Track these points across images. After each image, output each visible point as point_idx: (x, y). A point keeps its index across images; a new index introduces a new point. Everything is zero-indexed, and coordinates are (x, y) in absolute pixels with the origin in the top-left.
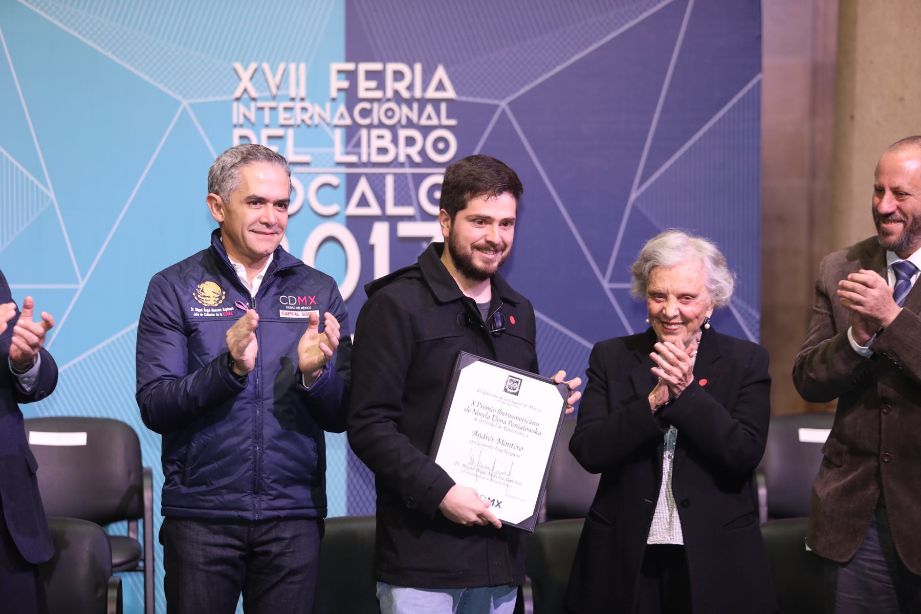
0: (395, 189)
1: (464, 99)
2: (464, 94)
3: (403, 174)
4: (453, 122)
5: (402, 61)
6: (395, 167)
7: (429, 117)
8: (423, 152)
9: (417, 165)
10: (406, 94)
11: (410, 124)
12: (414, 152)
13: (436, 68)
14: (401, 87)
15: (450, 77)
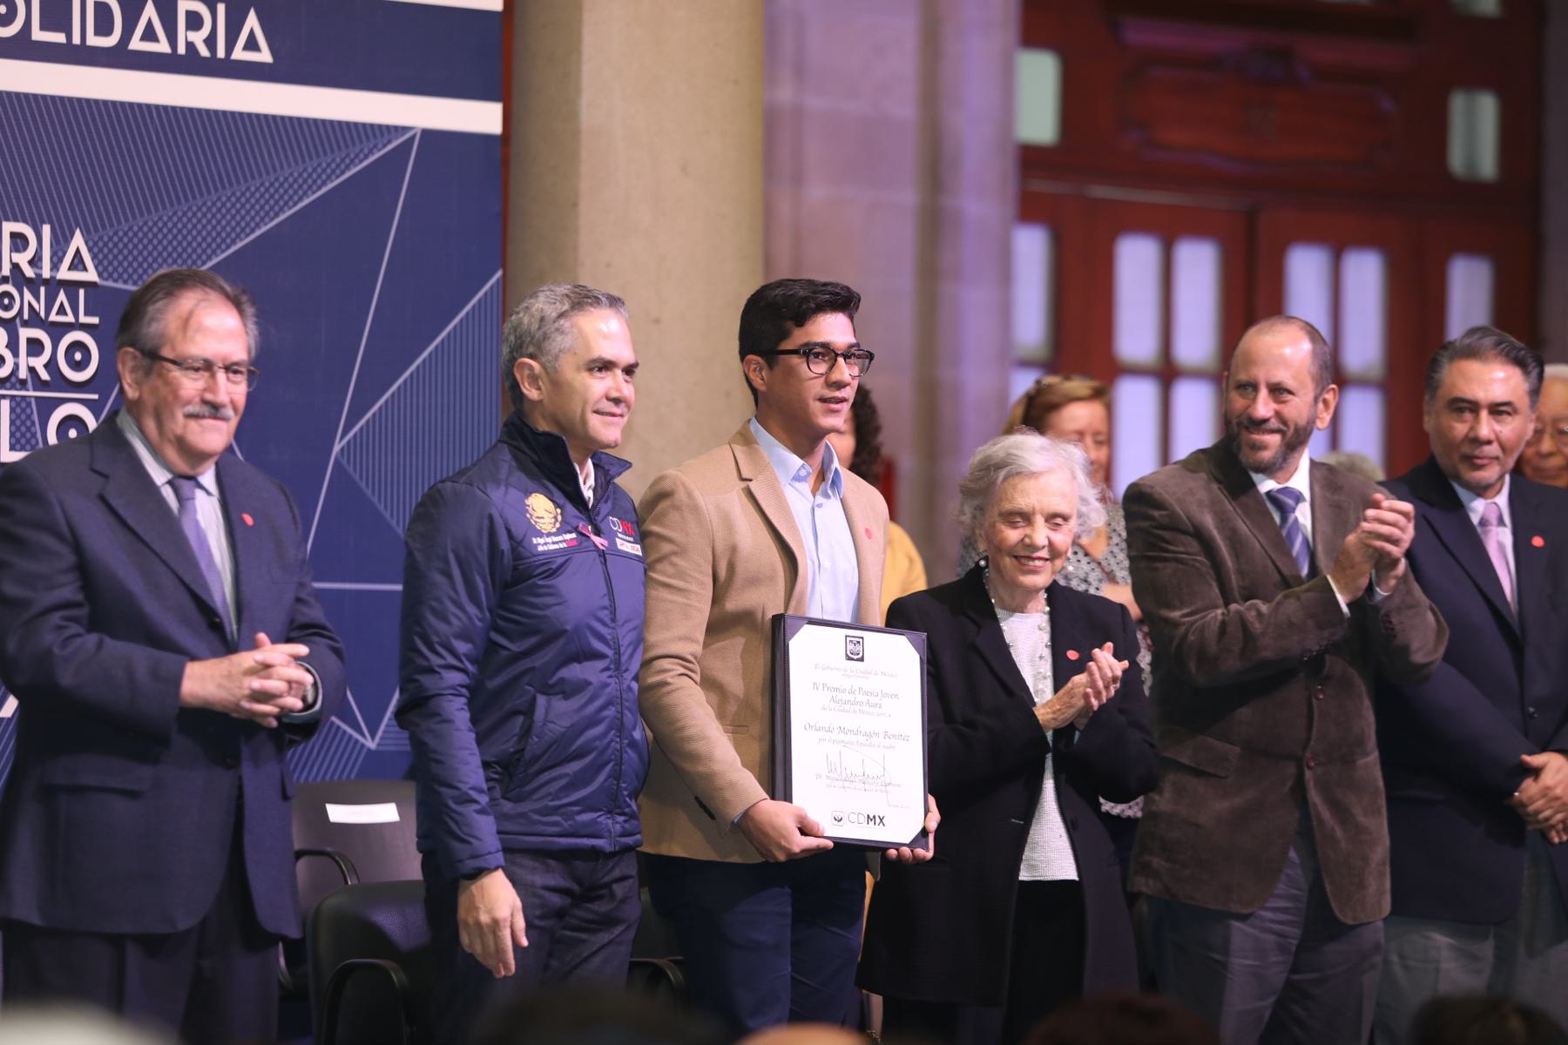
0: (12, 423)
1: (110, 284)
2: (110, 276)
3: (23, 397)
4: (95, 320)
5: (25, 221)
6: (13, 387)
7: (62, 311)
8: (51, 365)
9: (43, 385)
10: (29, 272)
11: (35, 320)
12: (39, 363)
13: (72, 235)
14: (22, 259)
15: (90, 250)
